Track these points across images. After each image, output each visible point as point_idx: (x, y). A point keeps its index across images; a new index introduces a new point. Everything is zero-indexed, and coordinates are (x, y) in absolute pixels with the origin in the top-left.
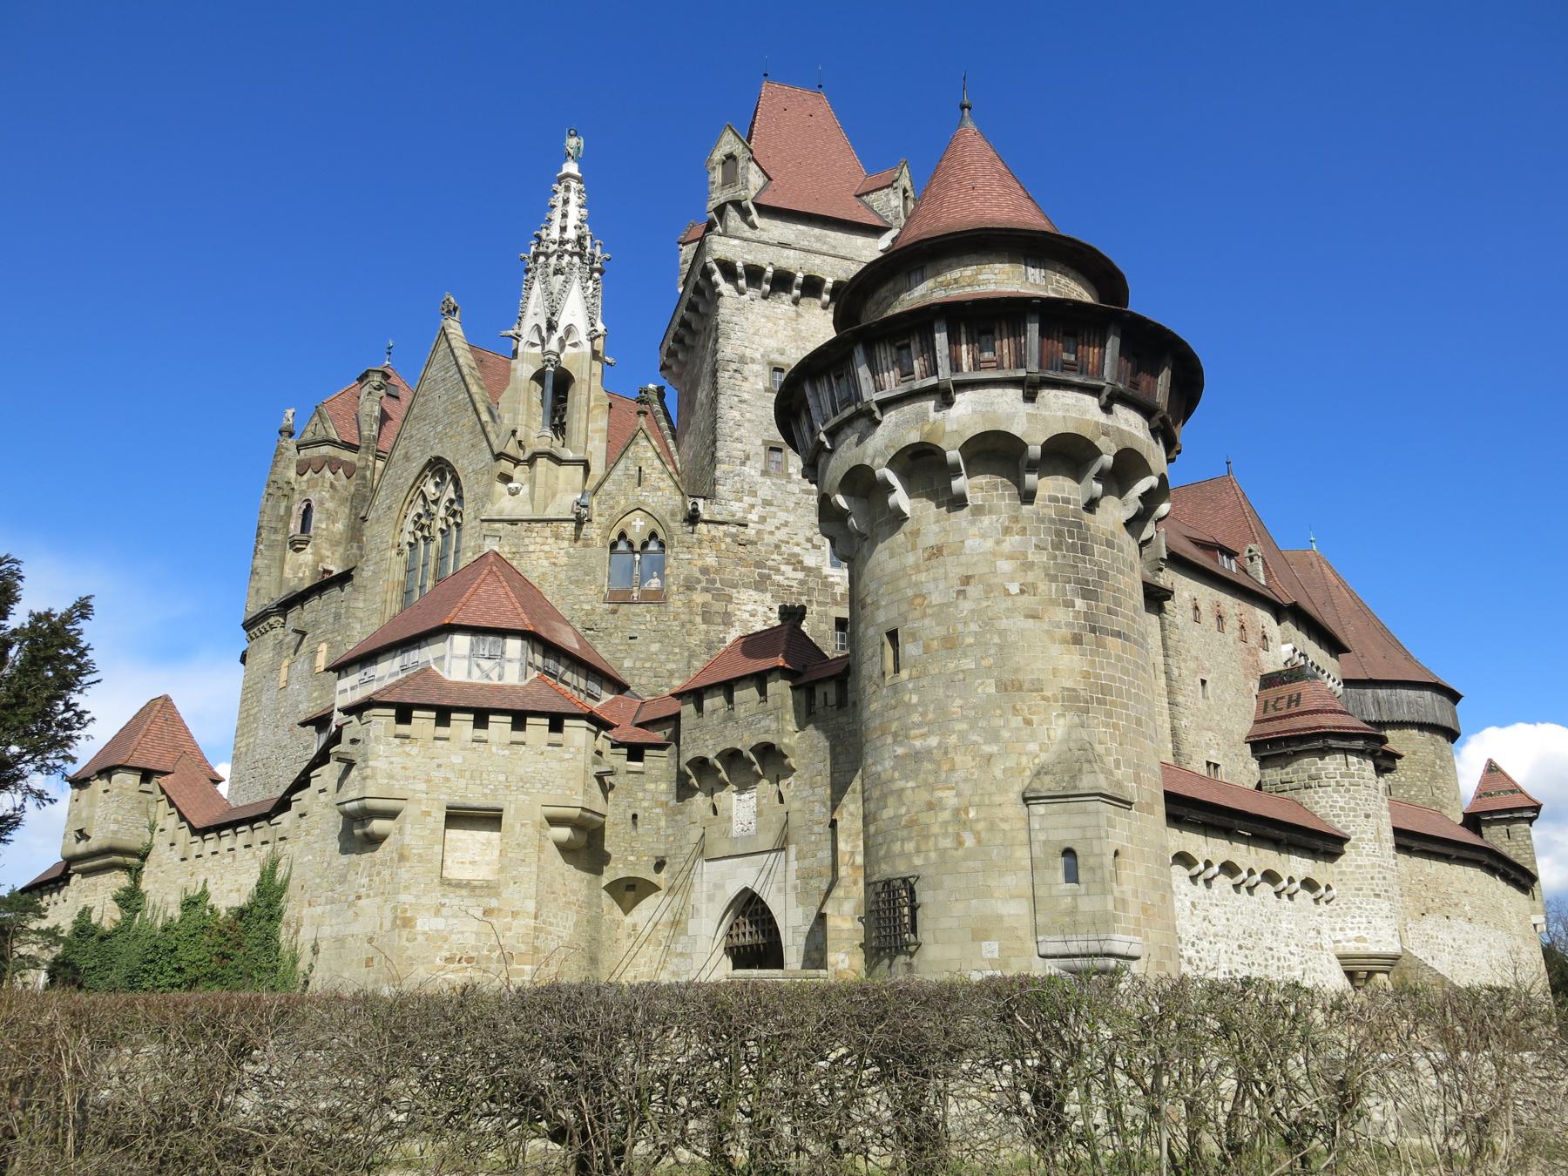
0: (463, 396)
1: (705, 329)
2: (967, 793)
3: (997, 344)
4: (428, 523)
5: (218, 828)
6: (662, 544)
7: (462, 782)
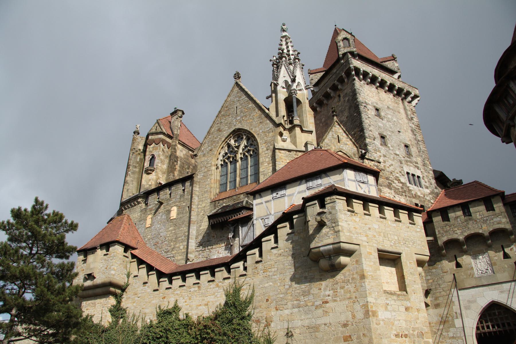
0: (251, 105)
1: (339, 96)
4: (232, 156)
5: (183, 274)
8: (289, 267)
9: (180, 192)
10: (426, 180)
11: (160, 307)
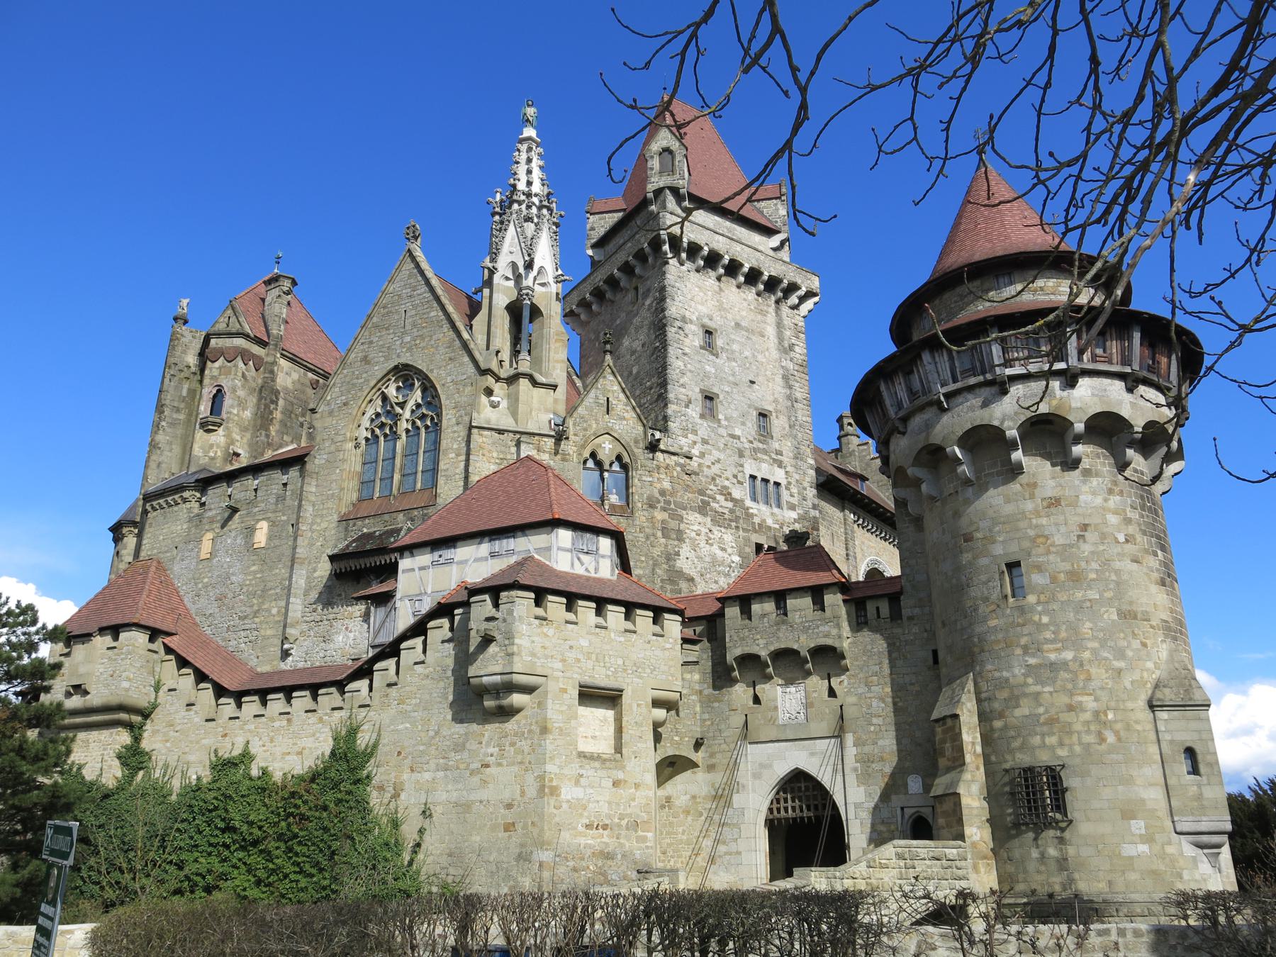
0: (436, 313)
1: (636, 289)
2: (1104, 699)
3: (1108, 343)
4: (389, 422)
6: (625, 467)
7: (590, 664)
8: (439, 700)
9: (276, 489)
10: (794, 490)
11: (216, 751)
